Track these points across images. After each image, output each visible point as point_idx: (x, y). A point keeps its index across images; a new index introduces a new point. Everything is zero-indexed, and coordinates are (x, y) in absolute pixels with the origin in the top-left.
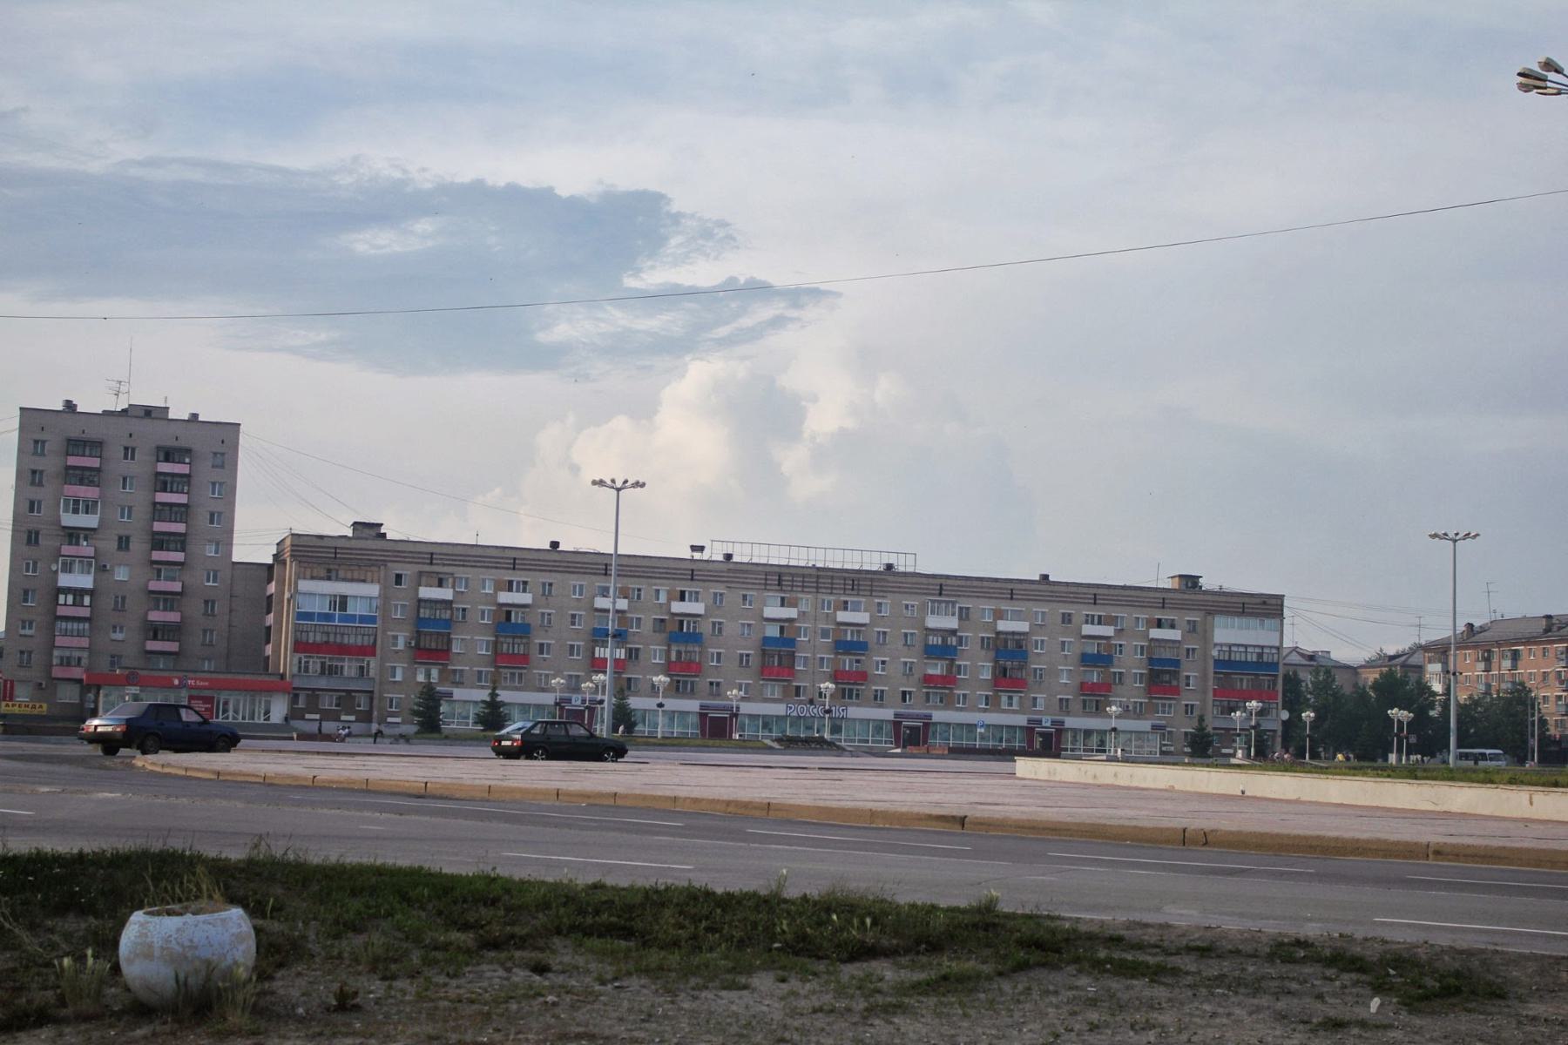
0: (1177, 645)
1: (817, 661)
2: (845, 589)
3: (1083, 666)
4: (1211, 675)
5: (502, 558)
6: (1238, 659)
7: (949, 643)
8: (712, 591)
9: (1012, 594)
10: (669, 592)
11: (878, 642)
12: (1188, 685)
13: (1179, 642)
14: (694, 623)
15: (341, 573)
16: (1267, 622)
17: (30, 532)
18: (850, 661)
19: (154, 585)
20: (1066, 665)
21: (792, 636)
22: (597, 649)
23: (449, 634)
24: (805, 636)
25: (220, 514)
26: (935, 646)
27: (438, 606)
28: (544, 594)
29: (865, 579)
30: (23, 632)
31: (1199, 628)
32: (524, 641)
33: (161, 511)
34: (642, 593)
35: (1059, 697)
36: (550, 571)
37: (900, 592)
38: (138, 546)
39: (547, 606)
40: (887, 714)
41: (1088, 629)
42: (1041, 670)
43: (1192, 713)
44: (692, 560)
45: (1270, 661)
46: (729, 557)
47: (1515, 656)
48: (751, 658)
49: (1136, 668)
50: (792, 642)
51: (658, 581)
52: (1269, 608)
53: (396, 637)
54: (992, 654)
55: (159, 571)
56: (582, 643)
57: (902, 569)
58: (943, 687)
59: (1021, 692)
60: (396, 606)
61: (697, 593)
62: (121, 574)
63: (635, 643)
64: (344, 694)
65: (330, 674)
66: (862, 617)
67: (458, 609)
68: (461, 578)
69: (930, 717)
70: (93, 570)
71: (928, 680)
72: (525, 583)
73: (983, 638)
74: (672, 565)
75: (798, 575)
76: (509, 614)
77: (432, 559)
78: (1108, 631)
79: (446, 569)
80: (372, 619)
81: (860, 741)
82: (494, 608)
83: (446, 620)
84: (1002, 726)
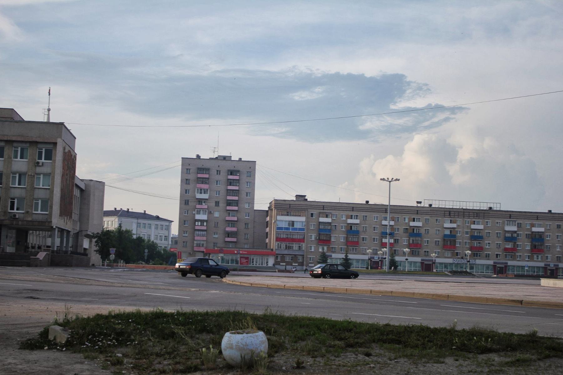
1: (464, 243)
2: (474, 217)
5: (349, 207)
7: (514, 236)
8: (425, 218)
9: (537, 218)
10: (409, 219)
11: (487, 236)
14: (418, 229)
15: (292, 214)
17: (186, 200)
18: (476, 243)
19: (228, 218)
20: (558, 244)
21: (455, 234)
22: (383, 239)
23: (330, 234)
24: (459, 234)
25: (250, 193)
26: (509, 237)
27: (326, 224)
28: (363, 220)
29: (481, 213)
30: (184, 235)
32: (357, 237)
33: (229, 192)
34: (399, 219)
35: (556, 256)
36: (366, 211)
37: (495, 217)
38: (222, 205)
39: (365, 225)
40: (491, 262)
42: (549, 246)
44: (417, 207)
46: (430, 205)
48: (439, 242)
50: (455, 236)
51: (405, 214)
53: (311, 236)
54: (531, 240)
55: (229, 213)
56: (378, 237)
57: (495, 209)
58: (512, 252)
59: (542, 254)
60: (311, 224)
61: (419, 219)
62: (217, 214)
64: (294, 256)
65: (289, 249)
66: (481, 227)
67: (333, 225)
68: (334, 214)
69: (507, 263)
70: (207, 213)
71: (506, 250)
72: (357, 216)
73: (526, 234)
74: (409, 208)
75: (456, 212)
76: (351, 227)
77: (324, 208)
79: (328, 211)
80: (303, 229)
81: (481, 272)
82: (346, 225)
83: (329, 229)
84: (535, 267)
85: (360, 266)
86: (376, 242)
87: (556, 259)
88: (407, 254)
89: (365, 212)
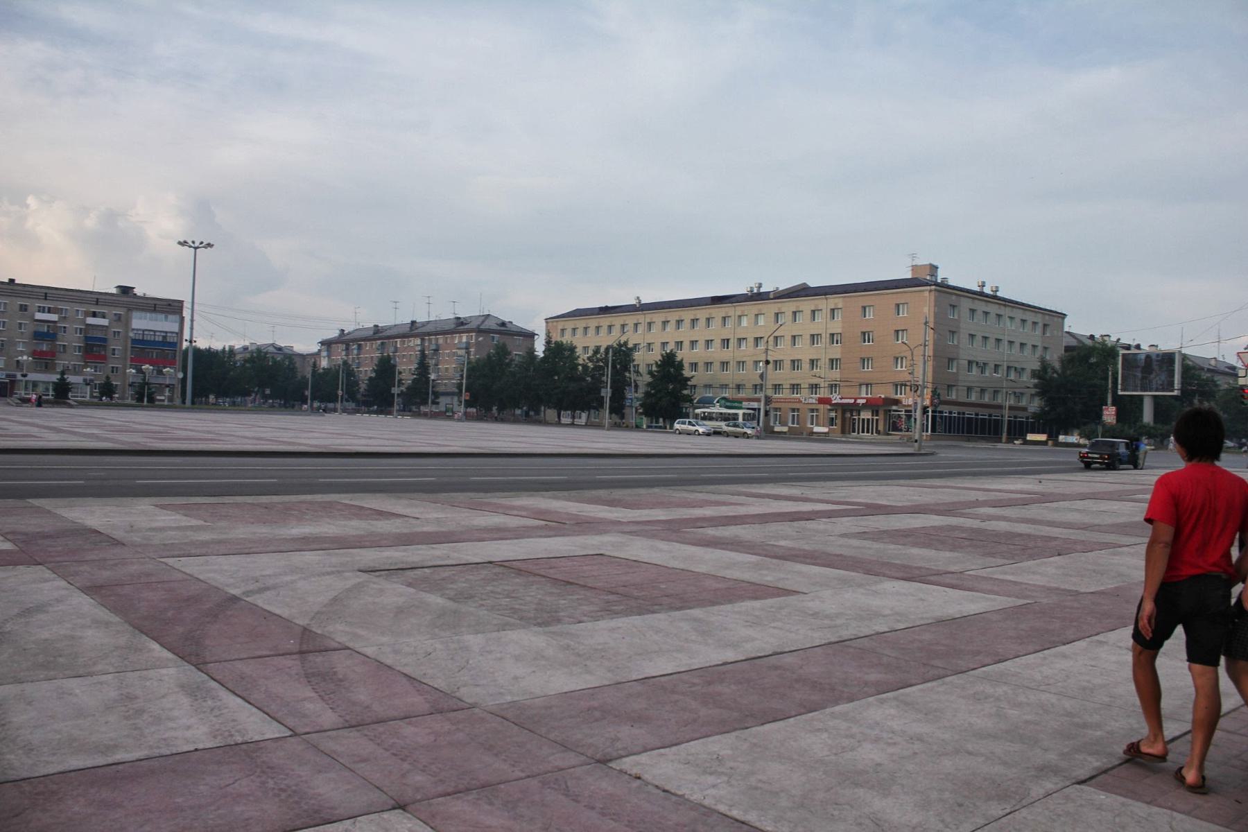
0: (105, 328)
3: (36, 339)
4: (129, 349)
6: (149, 339)
12: (114, 354)
13: (106, 326)
16: (170, 317)
31: (122, 319)
41: (39, 316)
43: (117, 372)
45: (172, 341)
47: (360, 347)
49: (75, 343)
52: (172, 308)
78: (54, 317)
81: (81, 397)
87: (15, 364)
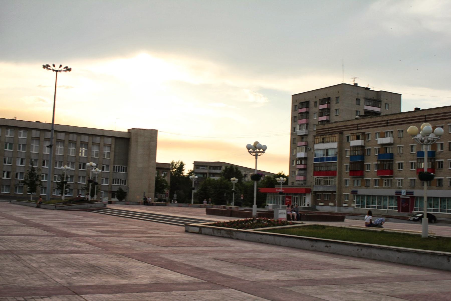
5: (382, 121)
63: (439, 159)
64: (331, 193)
85: (376, 206)
86: (414, 168)
88: (281, 184)
89: (399, 126)
